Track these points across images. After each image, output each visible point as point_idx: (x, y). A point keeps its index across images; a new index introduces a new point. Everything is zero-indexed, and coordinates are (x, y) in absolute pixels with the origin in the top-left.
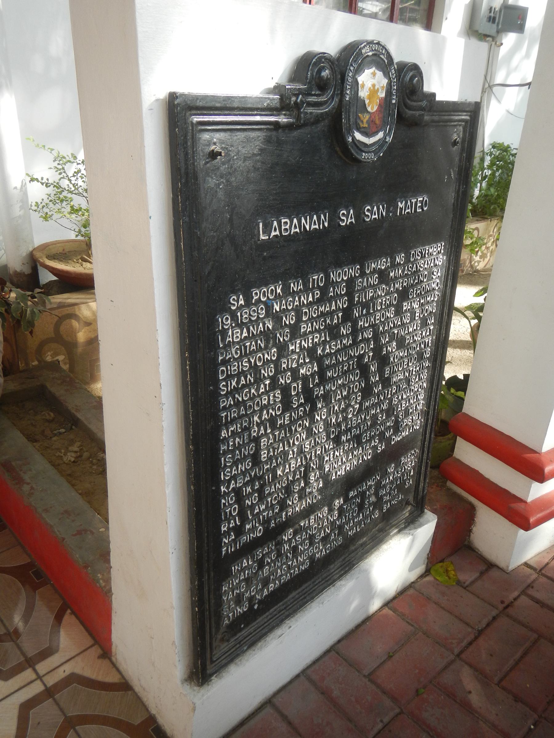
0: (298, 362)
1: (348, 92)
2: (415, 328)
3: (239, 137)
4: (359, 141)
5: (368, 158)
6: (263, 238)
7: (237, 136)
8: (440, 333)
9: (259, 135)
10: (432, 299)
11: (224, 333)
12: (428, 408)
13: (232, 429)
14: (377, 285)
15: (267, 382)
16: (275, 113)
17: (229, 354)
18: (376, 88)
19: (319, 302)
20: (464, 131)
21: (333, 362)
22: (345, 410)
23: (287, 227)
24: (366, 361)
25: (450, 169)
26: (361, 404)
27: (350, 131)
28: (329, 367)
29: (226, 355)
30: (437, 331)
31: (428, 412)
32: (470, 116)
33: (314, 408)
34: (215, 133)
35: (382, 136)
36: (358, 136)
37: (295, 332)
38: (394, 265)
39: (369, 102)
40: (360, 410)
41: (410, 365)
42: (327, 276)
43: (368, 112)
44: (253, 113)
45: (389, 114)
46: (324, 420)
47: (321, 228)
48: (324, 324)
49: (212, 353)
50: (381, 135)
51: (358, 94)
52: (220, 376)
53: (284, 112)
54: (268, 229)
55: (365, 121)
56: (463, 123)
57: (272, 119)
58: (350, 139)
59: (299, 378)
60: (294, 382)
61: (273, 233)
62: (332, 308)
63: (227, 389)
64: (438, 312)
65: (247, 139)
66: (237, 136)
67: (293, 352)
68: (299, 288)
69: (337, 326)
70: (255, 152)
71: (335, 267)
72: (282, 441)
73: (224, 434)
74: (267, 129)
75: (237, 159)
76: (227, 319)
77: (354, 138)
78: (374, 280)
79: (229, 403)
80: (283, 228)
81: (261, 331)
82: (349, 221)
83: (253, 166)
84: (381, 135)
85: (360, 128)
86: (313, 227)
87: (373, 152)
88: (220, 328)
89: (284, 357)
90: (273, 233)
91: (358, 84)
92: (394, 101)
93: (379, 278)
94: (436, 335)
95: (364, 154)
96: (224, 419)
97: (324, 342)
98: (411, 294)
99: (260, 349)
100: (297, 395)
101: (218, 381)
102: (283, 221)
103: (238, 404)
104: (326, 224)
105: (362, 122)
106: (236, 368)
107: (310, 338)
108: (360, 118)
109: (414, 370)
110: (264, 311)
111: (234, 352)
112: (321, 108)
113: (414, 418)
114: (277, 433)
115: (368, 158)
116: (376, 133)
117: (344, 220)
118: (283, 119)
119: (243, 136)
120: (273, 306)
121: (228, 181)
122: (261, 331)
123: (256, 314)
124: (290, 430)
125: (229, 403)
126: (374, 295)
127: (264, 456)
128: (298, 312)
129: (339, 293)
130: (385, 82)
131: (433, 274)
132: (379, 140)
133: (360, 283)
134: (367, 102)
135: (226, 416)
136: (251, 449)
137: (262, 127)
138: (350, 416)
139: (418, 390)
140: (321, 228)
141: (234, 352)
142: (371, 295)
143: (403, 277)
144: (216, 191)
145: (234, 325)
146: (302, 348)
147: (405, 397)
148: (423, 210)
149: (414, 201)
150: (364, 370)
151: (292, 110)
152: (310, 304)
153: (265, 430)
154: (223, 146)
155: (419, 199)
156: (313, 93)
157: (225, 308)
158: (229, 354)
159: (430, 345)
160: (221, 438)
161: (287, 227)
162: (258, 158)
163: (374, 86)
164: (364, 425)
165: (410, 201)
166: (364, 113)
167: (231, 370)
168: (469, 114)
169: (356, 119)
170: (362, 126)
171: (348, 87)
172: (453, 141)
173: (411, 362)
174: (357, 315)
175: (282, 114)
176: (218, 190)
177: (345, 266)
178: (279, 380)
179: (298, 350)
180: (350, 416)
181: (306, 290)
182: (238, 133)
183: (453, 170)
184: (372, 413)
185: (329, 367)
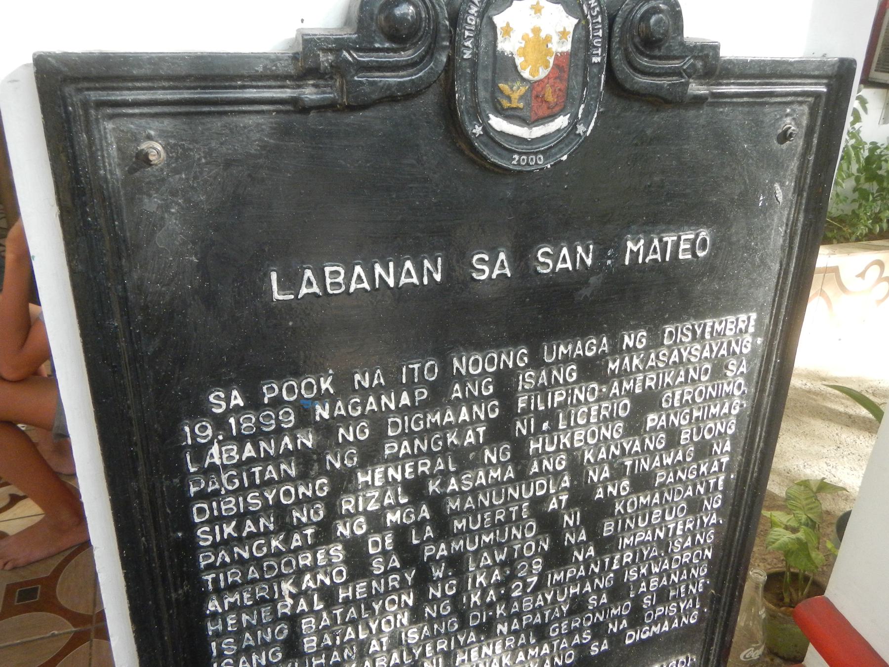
0: (380, 500)
1: (468, 43)
2: (680, 457)
3: (209, 126)
4: (501, 133)
5: (528, 164)
6: (281, 298)
7: (204, 124)
8: (747, 472)
9: (260, 121)
10: (725, 410)
11: (200, 451)
12: (720, 590)
13: (232, 600)
14: (574, 382)
15: (309, 531)
16: (288, 82)
17: (214, 483)
18: (543, 35)
19: (427, 406)
20: (813, 114)
21: (467, 506)
22: (506, 582)
23: (340, 279)
24: (551, 507)
25: (772, 182)
26: (542, 576)
27: (478, 114)
28: (458, 514)
29: (207, 485)
30: (740, 466)
31: (719, 600)
32: (827, 85)
33: (423, 581)
34: (149, 120)
35: (566, 123)
36: (498, 123)
37: (370, 454)
38: (616, 350)
39: (526, 61)
40: (540, 586)
41: (667, 518)
42: (445, 366)
43: (523, 80)
44: (233, 84)
45: (585, 84)
46: (453, 596)
47: (426, 282)
48: (440, 443)
49: (176, 480)
50: (562, 121)
51: (495, 46)
52: (195, 517)
53: (311, 82)
54: (291, 281)
55: (515, 96)
56: (810, 99)
57: (286, 93)
58: (478, 130)
59: (386, 528)
60: (375, 532)
61: (304, 291)
62: (461, 418)
63: (214, 538)
64: (744, 433)
65: (231, 130)
66: (204, 124)
67: (367, 485)
68: (376, 382)
69: (478, 448)
70: (253, 151)
71: (466, 350)
72: (354, 623)
73: (213, 605)
74: (278, 112)
75: (207, 163)
76: (204, 428)
77: (487, 128)
78: (571, 373)
79: (219, 560)
80: (328, 281)
81: (286, 449)
82: (496, 272)
83: (250, 176)
84: (562, 121)
85: (503, 109)
86: (404, 280)
87: (542, 152)
88: (190, 442)
89: (347, 491)
90: (304, 291)
91: (494, 27)
92: (596, 60)
93: (579, 371)
94: (739, 472)
95: (516, 157)
96: (210, 583)
97: (445, 475)
98: (667, 401)
99: (287, 479)
100: (385, 553)
101: (195, 526)
102: (327, 270)
103: (241, 562)
104: (438, 277)
105: (509, 98)
106: (231, 506)
107: (407, 466)
108: (502, 92)
109: (680, 527)
110: (292, 418)
111: (226, 483)
112: (401, 73)
113: (682, 606)
114: (338, 612)
115: (528, 164)
116: (552, 117)
117: (483, 271)
118: (309, 93)
119: (219, 124)
120: (315, 410)
121: (188, 200)
122: (286, 449)
123: (273, 422)
124: (369, 608)
125: (219, 560)
126: (566, 399)
127: (310, 644)
128: (378, 422)
129: (476, 394)
130: (571, 23)
131: (727, 368)
132: (559, 130)
133: (527, 379)
134: (519, 61)
135: (216, 581)
136: (283, 631)
137: (265, 108)
138: (515, 594)
139: (691, 560)
140: (426, 282)
141: (225, 481)
142: (558, 399)
143: (645, 371)
144: (163, 218)
145: (221, 438)
146: (388, 483)
147: (656, 570)
148: (694, 254)
149: (670, 239)
150: (549, 524)
151: (331, 78)
152: (402, 411)
153: (310, 604)
154: (172, 141)
155: (683, 237)
156: (377, 45)
157: (201, 411)
158: (214, 483)
159: (720, 488)
160: (208, 612)
161: (340, 279)
162: (261, 161)
163: (537, 31)
164: (553, 610)
165: (660, 241)
166: (514, 81)
167: (219, 509)
168: (825, 81)
169: (493, 93)
170: (506, 104)
171: (467, 33)
172: (780, 131)
173: (670, 513)
174: (524, 432)
175: (308, 85)
176: (166, 216)
177: (491, 347)
178: (336, 529)
179: (378, 483)
180: (515, 594)
181: (393, 385)
182: (207, 120)
183: (782, 185)
184: (572, 591)
185: (458, 514)
